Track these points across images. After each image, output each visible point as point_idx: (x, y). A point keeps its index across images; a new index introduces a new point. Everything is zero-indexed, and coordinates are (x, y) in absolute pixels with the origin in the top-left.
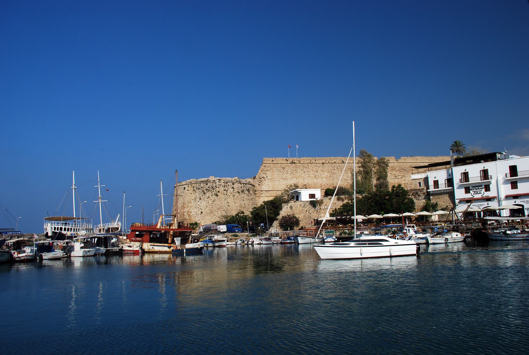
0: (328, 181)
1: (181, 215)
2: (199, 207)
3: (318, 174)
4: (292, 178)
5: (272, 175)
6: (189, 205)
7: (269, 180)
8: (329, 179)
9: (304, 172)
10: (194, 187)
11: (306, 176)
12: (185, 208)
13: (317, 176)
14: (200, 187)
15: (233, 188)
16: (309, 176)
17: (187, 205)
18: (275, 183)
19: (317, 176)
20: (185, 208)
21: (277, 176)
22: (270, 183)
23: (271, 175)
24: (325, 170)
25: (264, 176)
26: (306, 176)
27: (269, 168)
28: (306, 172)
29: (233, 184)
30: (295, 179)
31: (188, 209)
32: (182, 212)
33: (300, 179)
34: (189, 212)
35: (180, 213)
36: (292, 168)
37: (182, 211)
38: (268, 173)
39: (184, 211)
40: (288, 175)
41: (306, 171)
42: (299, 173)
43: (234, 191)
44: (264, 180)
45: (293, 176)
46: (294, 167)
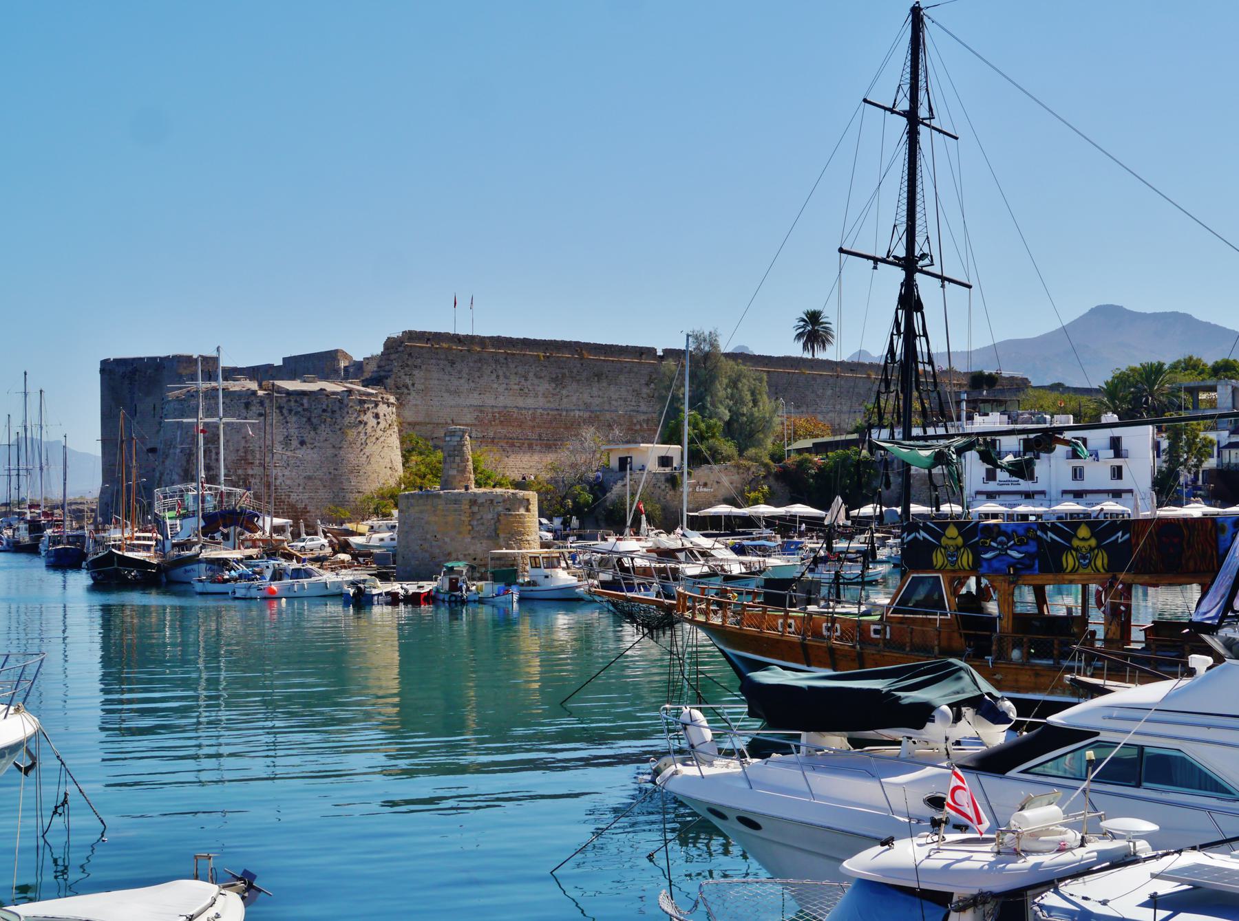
0: (549, 405)
3: (529, 383)
4: (471, 391)
5: (426, 379)
7: (418, 392)
8: (552, 400)
9: (498, 377)
10: (280, 408)
11: (501, 389)
12: (252, 463)
13: (527, 391)
14: (300, 409)
15: (377, 416)
16: (507, 389)
18: (432, 403)
19: (526, 391)
21: (436, 382)
22: (419, 402)
23: (423, 381)
24: (543, 375)
25: (409, 382)
26: (501, 389)
27: (419, 360)
28: (501, 378)
29: (376, 405)
30: (476, 395)
32: (242, 477)
33: (488, 394)
36: (472, 364)
37: (240, 472)
38: (416, 372)
39: (250, 472)
40: (462, 381)
41: (501, 373)
42: (486, 377)
43: (378, 423)
44: (406, 391)
45: (472, 385)
46: (475, 362)
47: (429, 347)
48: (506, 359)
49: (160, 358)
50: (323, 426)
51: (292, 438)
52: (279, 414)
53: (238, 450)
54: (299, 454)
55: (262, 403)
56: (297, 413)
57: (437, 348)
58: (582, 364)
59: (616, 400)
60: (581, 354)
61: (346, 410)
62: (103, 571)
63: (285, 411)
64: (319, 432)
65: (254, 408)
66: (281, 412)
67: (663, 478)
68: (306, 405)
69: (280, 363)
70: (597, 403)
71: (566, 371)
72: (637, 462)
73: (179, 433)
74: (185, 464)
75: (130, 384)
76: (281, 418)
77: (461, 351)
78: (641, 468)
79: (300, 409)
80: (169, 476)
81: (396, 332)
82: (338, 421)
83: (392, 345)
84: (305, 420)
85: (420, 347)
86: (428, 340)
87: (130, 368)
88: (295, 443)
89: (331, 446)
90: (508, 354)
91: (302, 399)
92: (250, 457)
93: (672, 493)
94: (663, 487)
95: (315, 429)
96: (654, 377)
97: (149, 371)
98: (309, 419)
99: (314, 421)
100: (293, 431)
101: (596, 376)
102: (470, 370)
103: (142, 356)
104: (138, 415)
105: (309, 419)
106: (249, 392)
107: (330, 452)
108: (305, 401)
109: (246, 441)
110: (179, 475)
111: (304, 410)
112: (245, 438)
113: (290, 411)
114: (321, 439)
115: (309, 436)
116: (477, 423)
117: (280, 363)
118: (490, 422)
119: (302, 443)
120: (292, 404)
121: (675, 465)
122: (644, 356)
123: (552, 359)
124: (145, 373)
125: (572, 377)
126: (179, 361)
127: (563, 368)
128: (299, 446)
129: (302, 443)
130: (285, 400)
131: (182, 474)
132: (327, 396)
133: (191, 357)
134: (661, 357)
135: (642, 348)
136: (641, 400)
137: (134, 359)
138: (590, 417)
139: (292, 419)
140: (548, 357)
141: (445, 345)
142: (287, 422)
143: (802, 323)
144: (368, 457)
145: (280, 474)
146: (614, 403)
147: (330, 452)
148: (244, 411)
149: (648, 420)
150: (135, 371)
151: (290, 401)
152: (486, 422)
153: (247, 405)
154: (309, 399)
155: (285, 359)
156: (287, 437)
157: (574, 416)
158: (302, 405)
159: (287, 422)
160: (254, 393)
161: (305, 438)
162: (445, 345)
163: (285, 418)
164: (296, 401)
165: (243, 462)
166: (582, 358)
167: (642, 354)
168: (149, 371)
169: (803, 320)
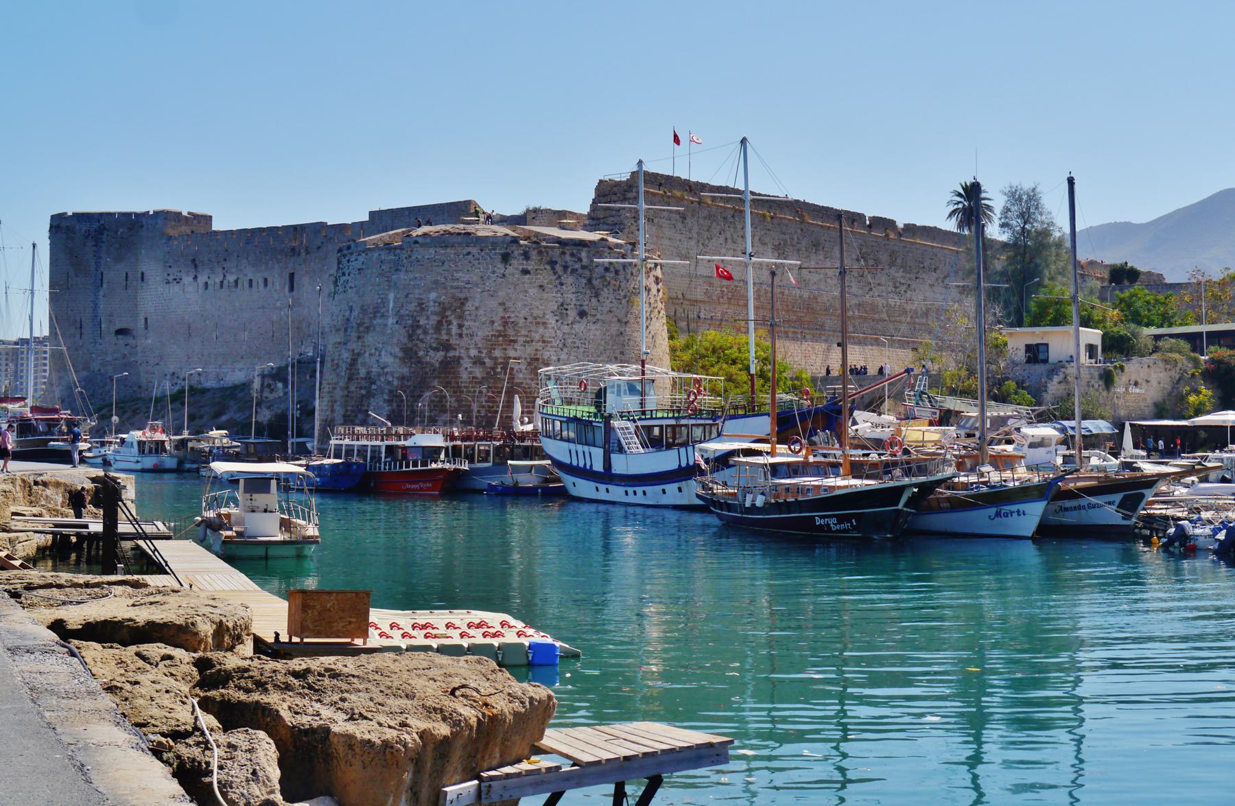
1: (493, 369)
2: (578, 343)
6: (536, 332)
10: (552, 263)
14: (577, 266)
17: (523, 332)
20: (515, 341)
21: (667, 242)
28: (729, 241)
31: (530, 350)
32: (500, 360)
34: (537, 359)
35: (487, 360)
36: (701, 221)
37: (497, 353)
40: (693, 243)
42: (714, 240)
47: (662, 196)
48: (733, 216)
49: (136, 214)
50: (605, 290)
51: (569, 307)
52: (551, 272)
53: (493, 322)
54: (580, 327)
55: (526, 256)
56: (574, 271)
57: (669, 197)
58: (802, 230)
59: (831, 278)
60: (801, 216)
61: (630, 269)
62: (858, 517)
63: (558, 268)
64: (601, 298)
65: (514, 262)
66: (553, 269)
67: (1096, 374)
68: (585, 261)
69: (366, 218)
70: (815, 280)
71: (787, 237)
72: (1055, 353)
73: (391, 296)
74: (405, 340)
75: (96, 246)
76: (554, 277)
77: (692, 202)
78: (1069, 359)
79: (577, 266)
80: (373, 359)
81: (620, 172)
82: (623, 285)
83: (607, 191)
84: (584, 281)
85: (652, 193)
86: (660, 185)
87: (96, 226)
88: (572, 314)
89: (616, 319)
90: (736, 211)
91: (579, 251)
92: (510, 332)
93: (1105, 393)
94: (1096, 386)
95: (597, 295)
96: (864, 250)
97: (121, 230)
98: (590, 281)
99: (596, 283)
100: (570, 297)
101: (815, 245)
102: (700, 229)
103: (112, 210)
104: (105, 286)
105: (590, 281)
106: (508, 238)
107: (615, 328)
108: (584, 255)
109: (505, 309)
110: (395, 357)
111: (583, 267)
112: (504, 304)
113: (565, 268)
114: (606, 309)
115: (589, 304)
116: (706, 299)
117: (366, 218)
118: (718, 299)
119: (582, 314)
120: (568, 258)
121: (1099, 358)
122: (855, 223)
123: (775, 221)
124: (116, 232)
125: (793, 246)
126: (165, 219)
127: (784, 234)
128: (577, 318)
129: (582, 314)
130: (557, 252)
131: (400, 354)
132: (610, 248)
133: (180, 213)
134: (870, 226)
135: (853, 213)
136: (853, 279)
137: (101, 214)
138: (809, 298)
139: (569, 279)
140: (772, 218)
141: (678, 194)
142: (562, 284)
143: (959, 199)
144: (653, 337)
145: (554, 358)
146: (829, 280)
147: (615, 328)
148: (501, 266)
149: (859, 305)
150: (101, 230)
151: (564, 253)
152: (715, 298)
153: (506, 258)
154: (589, 252)
155: (372, 214)
156: (562, 305)
157: (795, 296)
158: (580, 260)
159: (562, 284)
160: (515, 241)
161: (585, 308)
162: (678, 194)
163: (559, 277)
164: (572, 255)
165: (501, 339)
166: (802, 222)
167: (853, 221)
168: (121, 230)
169: (960, 195)
